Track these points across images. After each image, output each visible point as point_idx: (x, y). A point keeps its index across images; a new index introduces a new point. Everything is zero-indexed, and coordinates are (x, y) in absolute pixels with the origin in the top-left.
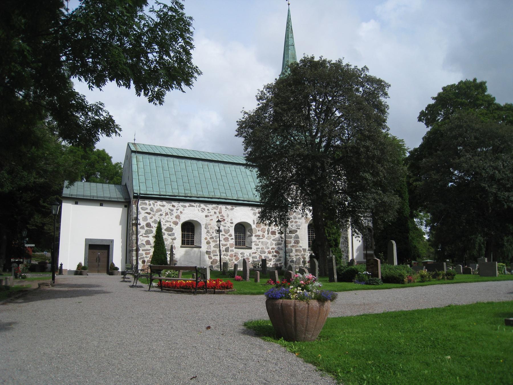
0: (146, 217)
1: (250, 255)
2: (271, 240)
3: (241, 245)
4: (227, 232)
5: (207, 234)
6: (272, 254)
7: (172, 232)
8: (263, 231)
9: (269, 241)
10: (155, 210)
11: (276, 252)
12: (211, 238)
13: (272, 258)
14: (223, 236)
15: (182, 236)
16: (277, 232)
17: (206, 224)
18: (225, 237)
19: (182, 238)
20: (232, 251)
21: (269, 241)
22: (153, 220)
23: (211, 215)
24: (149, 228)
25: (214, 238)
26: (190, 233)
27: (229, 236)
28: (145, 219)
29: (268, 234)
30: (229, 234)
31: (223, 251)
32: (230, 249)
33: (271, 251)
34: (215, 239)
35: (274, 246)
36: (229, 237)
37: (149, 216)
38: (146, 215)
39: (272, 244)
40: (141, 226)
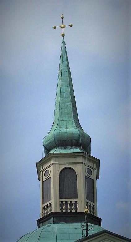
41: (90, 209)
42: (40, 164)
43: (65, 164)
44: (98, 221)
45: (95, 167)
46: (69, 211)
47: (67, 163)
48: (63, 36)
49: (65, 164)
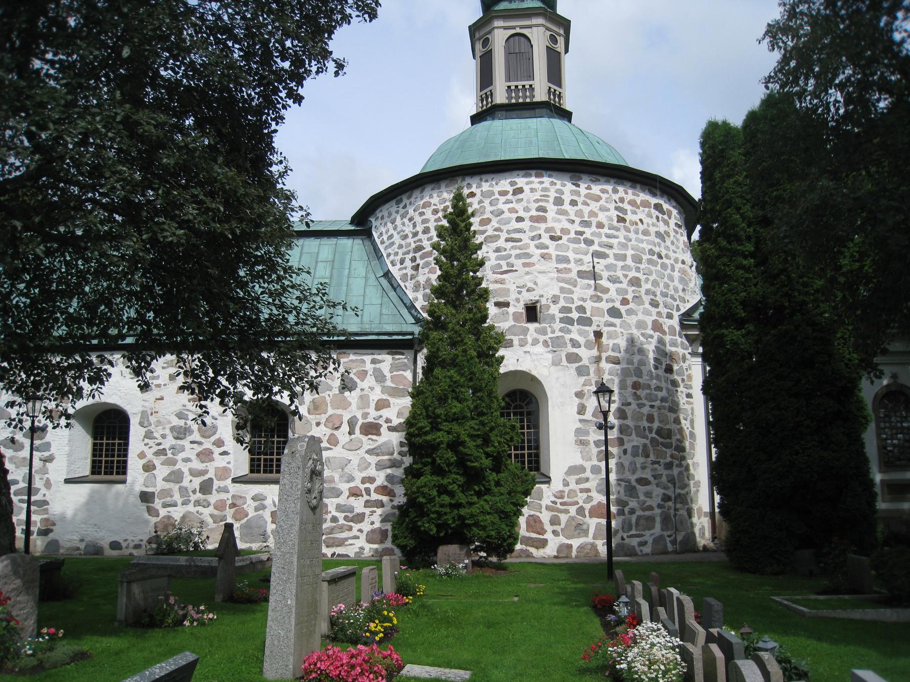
2: (362, 452)
4: (207, 434)
5: (147, 441)
6: (366, 497)
7: (44, 441)
8: (330, 425)
9: (355, 458)
14: (195, 446)
15: (94, 450)
16: (385, 426)
17: (144, 415)
18: (201, 449)
19: (94, 455)
20: (225, 490)
21: (355, 458)
23: (159, 386)
25: (169, 452)
26: (117, 441)
27: (214, 444)
29: (350, 433)
30: (213, 439)
31: (194, 492)
32: (216, 484)
33: (362, 487)
34: (170, 455)
35: (372, 472)
39: (364, 466)
41: (555, 98)
42: (474, 29)
43: (514, 28)
44: (566, 115)
45: (562, 32)
46: (521, 100)
49: (514, 28)
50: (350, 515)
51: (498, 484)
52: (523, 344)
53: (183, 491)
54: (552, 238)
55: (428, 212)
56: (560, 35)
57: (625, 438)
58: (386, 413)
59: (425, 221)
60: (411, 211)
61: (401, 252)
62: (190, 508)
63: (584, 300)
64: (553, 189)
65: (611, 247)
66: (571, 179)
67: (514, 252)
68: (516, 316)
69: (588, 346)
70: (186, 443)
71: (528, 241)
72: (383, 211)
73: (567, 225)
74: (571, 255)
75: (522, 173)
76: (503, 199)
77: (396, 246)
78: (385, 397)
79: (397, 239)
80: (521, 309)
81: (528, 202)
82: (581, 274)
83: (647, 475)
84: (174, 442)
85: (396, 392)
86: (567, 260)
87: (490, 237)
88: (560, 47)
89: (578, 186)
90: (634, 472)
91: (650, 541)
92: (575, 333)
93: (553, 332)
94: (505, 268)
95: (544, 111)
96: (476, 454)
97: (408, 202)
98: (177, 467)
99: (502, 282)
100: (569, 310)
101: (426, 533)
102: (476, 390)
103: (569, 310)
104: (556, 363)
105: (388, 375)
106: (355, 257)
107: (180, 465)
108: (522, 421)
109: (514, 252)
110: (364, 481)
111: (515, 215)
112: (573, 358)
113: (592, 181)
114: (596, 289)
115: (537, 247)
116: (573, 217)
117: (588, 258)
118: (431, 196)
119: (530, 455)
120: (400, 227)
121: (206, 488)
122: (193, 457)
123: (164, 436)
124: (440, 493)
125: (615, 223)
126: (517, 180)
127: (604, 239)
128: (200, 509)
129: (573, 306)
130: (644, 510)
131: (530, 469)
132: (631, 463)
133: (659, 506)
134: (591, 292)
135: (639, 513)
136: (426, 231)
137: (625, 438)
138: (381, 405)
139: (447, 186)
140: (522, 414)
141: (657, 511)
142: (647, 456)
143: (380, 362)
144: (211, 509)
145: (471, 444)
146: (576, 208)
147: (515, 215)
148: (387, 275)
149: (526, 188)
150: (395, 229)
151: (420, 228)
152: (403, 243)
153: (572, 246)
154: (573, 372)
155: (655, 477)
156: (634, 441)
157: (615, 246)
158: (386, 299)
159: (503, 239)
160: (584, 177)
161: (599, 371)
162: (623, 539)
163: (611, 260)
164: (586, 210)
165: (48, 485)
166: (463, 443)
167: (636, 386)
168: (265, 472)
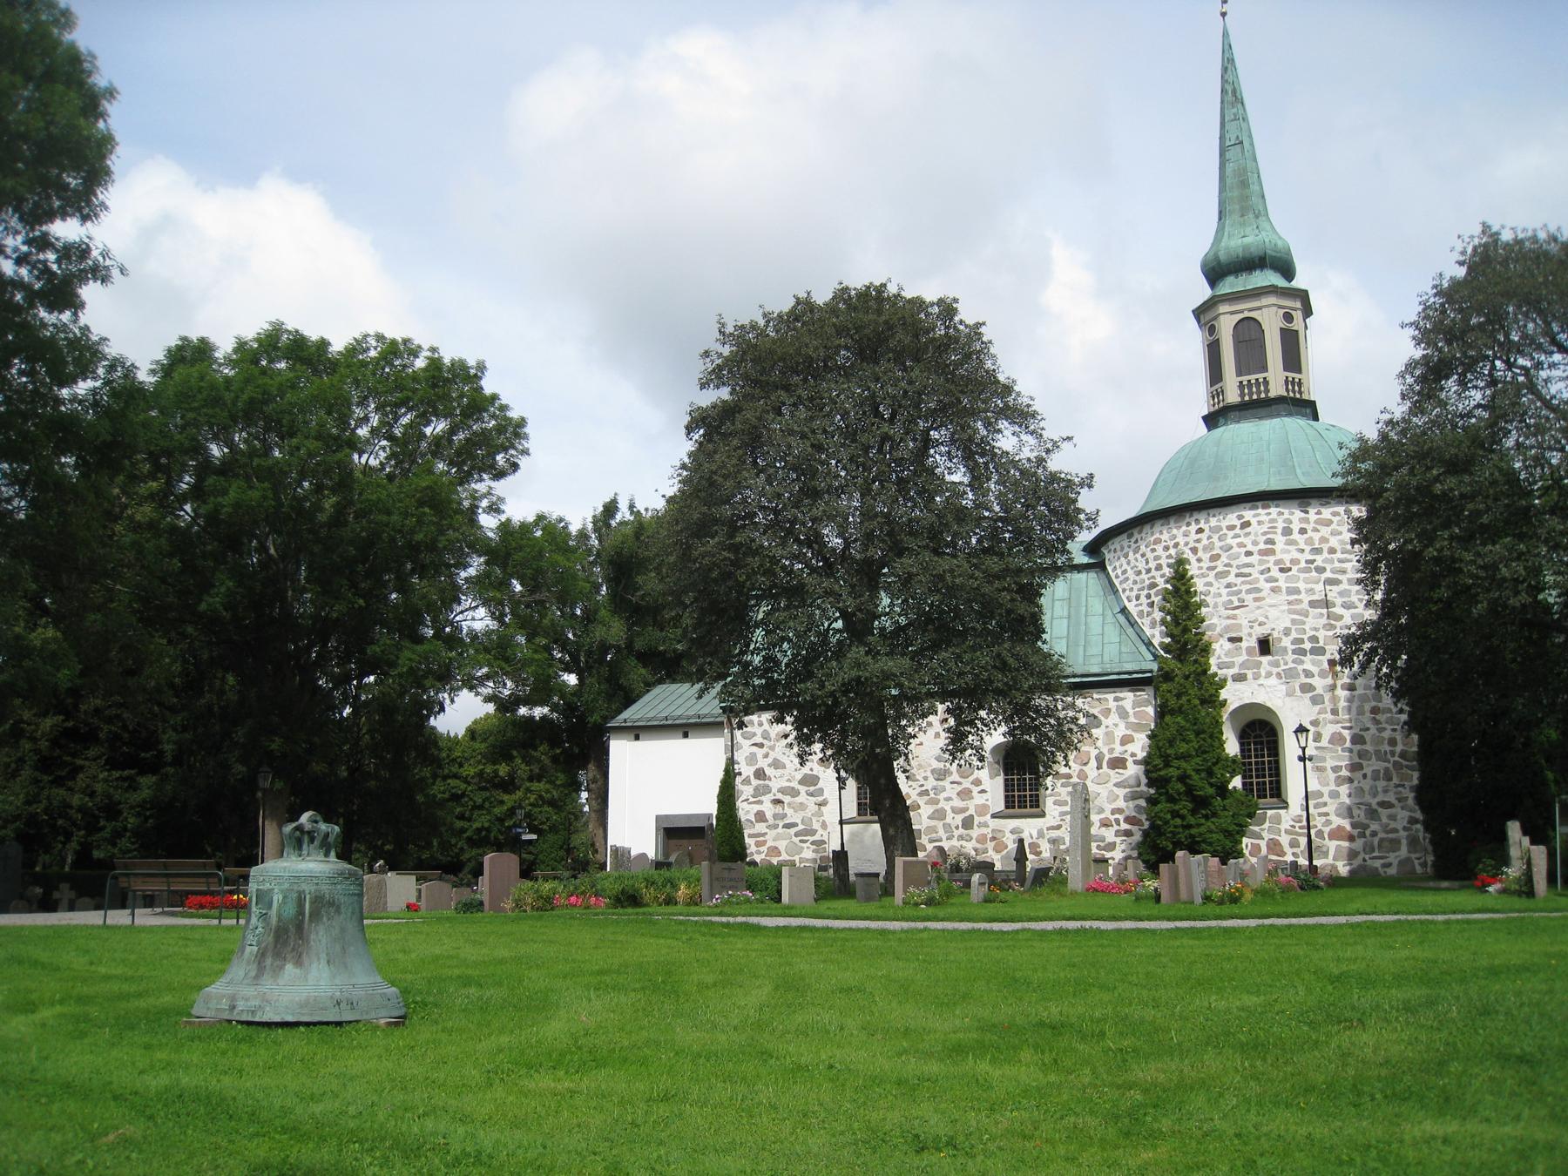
0: (753, 755)
1: (1041, 834)
2: (1110, 785)
3: (1025, 807)
6: (1116, 827)
10: (773, 736)
11: (1127, 820)
12: (921, 794)
13: (1118, 840)
15: (859, 794)
16: (1130, 760)
22: (770, 760)
24: (761, 782)
28: (752, 759)
30: (971, 779)
32: (977, 820)
33: (1112, 818)
34: (932, 795)
35: (1121, 804)
36: (973, 787)
37: (760, 752)
38: (755, 749)
40: (743, 777)
42: (1199, 313)
43: (1241, 311)
44: (1308, 409)
45: (1298, 305)
46: (1255, 397)
47: (1245, 308)
48: (1224, 14)
49: (1241, 311)
50: (1102, 844)
51: (1225, 809)
52: (1256, 677)
53: (947, 827)
54: (1281, 570)
55: (1159, 548)
56: (1295, 309)
57: (1365, 763)
58: (1130, 748)
59: (1157, 558)
60: (1143, 547)
61: (1136, 587)
62: (955, 842)
63: (1316, 629)
64: (1280, 519)
65: (1344, 572)
66: (1300, 506)
67: (1245, 587)
68: (1249, 651)
69: (1322, 674)
70: (946, 783)
71: (1258, 575)
72: (1115, 544)
73: (1297, 555)
74: (1301, 585)
75: (1250, 505)
76: (1231, 534)
77: (1130, 582)
78: (1129, 732)
79: (1130, 573)
80: (1254, 643)
81: (1256, 535)
82: (1313, 604)
83: (1391, 798)
84: (935, 783)
85: (1138, 727)
86: (1297, 591)
87: (1221, 573)
88: (1298, 324)
89: (1307, 512)
90: (1375, 795)
91: (1395, 863)
92: (1308, 663)
93: (1286, 664)
94: (1236, 604)
95: (1281, 407)
96: (1200, 784)
97: (1139, 537)
98: (940, 806)
99: (1234, 617)
100: (1302, 641)
101: (1163, 849)
102: (1198, 733)
103: (1302, 641)
104: (1290, 694)
105: (1131, 712)
106: (1091, 593)
107: (942, 804)
108: (1262, 750)
109: (1245, 587)
110: (1113, 812)
111: (1243, 550)
112: (1307, 688)
113: (1322, 505)
114: (1328, 617)
115: (1267, 581)
116: (1302, 546)
117: (1320, 586)
118: (1161, 532)
119: (1271, 782)
120: (1133, 561)
121: (968, 823)
122: (954, 796)
123: (926, 778)
124: (1173, 818)
125: (1349, 547)
126: (1243, 513)
127: (1337, 564)
128: (964, 843)
129: (1305, 637)
130: (1387, 832)
131: (1259, 797)
132: (1371, 788)
133: (1405, 829)
134: (1324, 621)
135: (1382, 835)
136: (1159, 568)
137: (1365, 763)
138: (1126, 740)
139: (1176, 522)
140: (1262, 743)
141: (1403, 834)
142: (1390, 779)
143: (1122, 699)
144: (973, 843)
145: (1196, 777)
146: (1305, 536)
147: (1243, 550)
148: (1124, 611)
149: (1254, 521)
150: (1128, 563)
151: (1152, 565)
152: (1137, 578)
153: (1302, 576)
154: (1308, 702)
155: (1399, 800)
156: (1371, 766)
157: (1349, 570)
158: (1124, 637)
159: (1233, 574)
160: (1313, 502)
161: (1334, 699)
162: (1364, 860)
163: (1344, 586)
164: (1316, 536)
165: (824, 826)
166: (1189, 777)
167: (1375, 711)
168: (1019, 807)
